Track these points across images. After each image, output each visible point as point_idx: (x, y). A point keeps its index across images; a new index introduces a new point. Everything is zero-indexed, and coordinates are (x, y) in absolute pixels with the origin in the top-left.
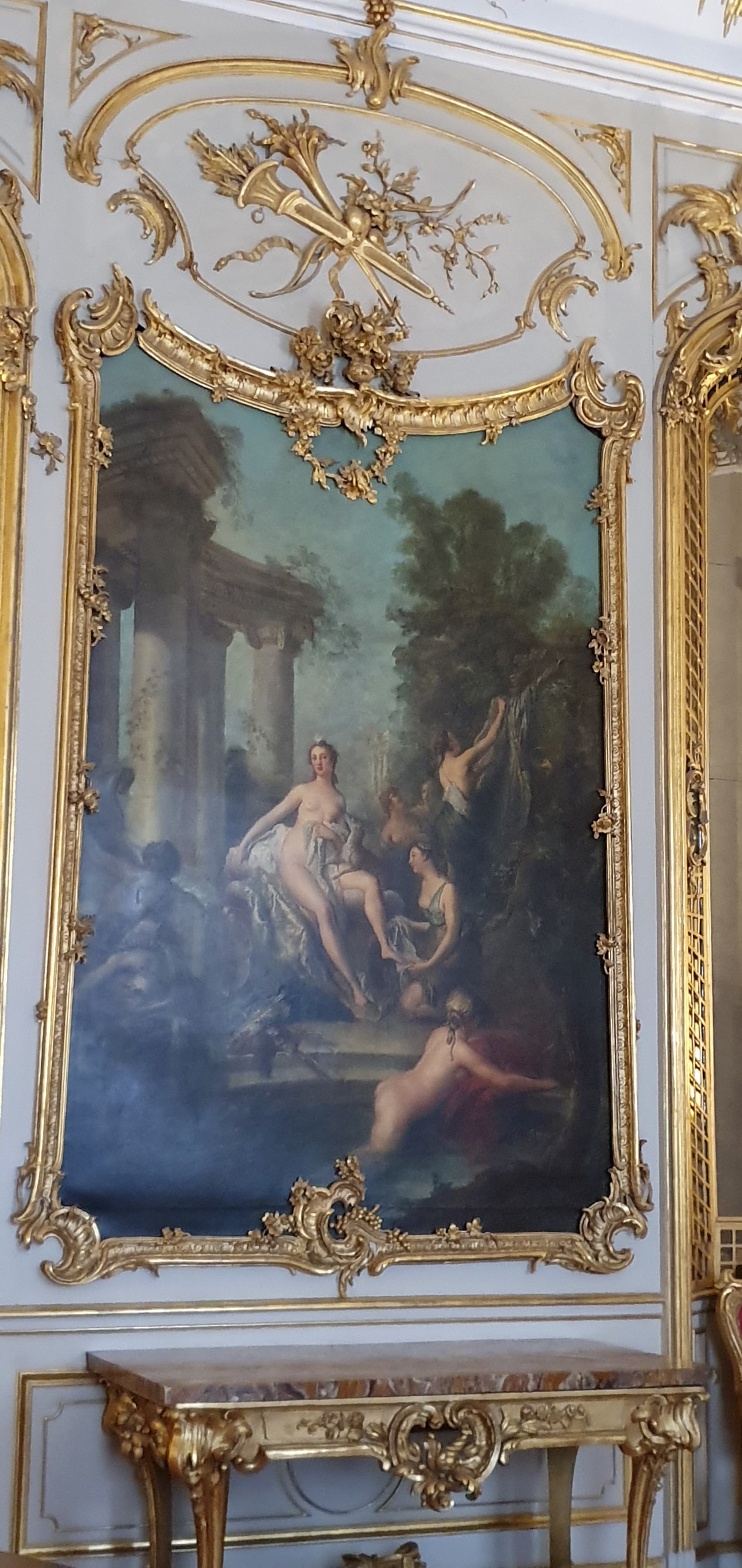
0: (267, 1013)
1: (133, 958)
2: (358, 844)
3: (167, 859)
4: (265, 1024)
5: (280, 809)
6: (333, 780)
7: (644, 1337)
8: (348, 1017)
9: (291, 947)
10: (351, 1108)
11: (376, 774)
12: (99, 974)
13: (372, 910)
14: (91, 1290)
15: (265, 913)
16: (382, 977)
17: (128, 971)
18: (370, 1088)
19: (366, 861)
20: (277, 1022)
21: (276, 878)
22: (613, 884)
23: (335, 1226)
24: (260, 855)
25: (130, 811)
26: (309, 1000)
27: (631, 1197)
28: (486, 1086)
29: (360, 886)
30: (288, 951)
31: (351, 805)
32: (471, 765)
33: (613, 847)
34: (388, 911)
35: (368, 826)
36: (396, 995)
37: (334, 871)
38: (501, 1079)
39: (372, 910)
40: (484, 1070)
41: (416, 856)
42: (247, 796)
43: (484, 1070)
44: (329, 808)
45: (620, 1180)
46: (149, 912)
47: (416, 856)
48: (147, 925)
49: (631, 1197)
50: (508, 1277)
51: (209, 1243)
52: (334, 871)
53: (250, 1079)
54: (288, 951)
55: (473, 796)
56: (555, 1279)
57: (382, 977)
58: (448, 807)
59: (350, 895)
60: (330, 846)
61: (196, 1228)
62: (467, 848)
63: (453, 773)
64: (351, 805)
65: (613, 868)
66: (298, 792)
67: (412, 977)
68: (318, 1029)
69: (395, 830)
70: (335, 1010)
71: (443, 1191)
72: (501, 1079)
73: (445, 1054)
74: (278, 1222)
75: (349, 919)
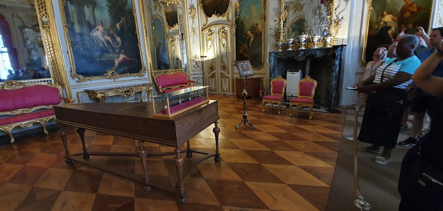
0: (99, 52)
1: (80, 46)
2: (107, 33)
3: (81, 35)
4: (99, 54)
5: (96, 29)
6: (102, 25)
7: (147, 82)
8: (110, 53)
9: (101, 45)
10: (112, 63)
11: (108, 26)
12: (75, 48)
13: (110, 41)
14: (83, 83)
15: (97, 41)
16: (113, 48)
17: (79, 48)
18: (114, 60)
19: (108, 35)
20: (101, 53)
21: (97, 37)
22: (138, 38)
23: (112, 74)
24: (94, 34)
25: (74, 28)
26: (104, 51)
27: (144, 69)
28: (127, 59)
29: (109, 38)
30: (101, 45)
31: (106, 28)
32: (120, 25)
33: (138, 35)
34: (112, 41)
35: (108, 31)
36: (115, 50)
37: (105, 36)
38: (129, 59)
39: (110, 41)
40: (127, 58)
41: (115, 35)
42: (91, 27)
43: (127, 58)
44: (102, 29)
45: (143, 68)
46: (80, 41)
47: (115, 35)
48: (81, 43)
49: (144, 69)
50: (133, 78)
51: (97, 77)
52: (105, 36)
53: (99, 60)
54: (101, 45)
55: (120, 28)
56: (137, 78)
57: (113, 48)
58: (118, 29)
59: (107, 39)
60: (104, 34)
61: (96, 76)
62: (121, 34)
63: (118, 25)
64: (106, 28)
65: (138, 37)
66: (98, 27)
67: (117, 48)
68: (106, 54)
69: (111, 32)
70: (108, 52)
71: (124, 70)
72: (129, 59)
73: (122, 57)
74: (106, 74)
75: (108, 42)
